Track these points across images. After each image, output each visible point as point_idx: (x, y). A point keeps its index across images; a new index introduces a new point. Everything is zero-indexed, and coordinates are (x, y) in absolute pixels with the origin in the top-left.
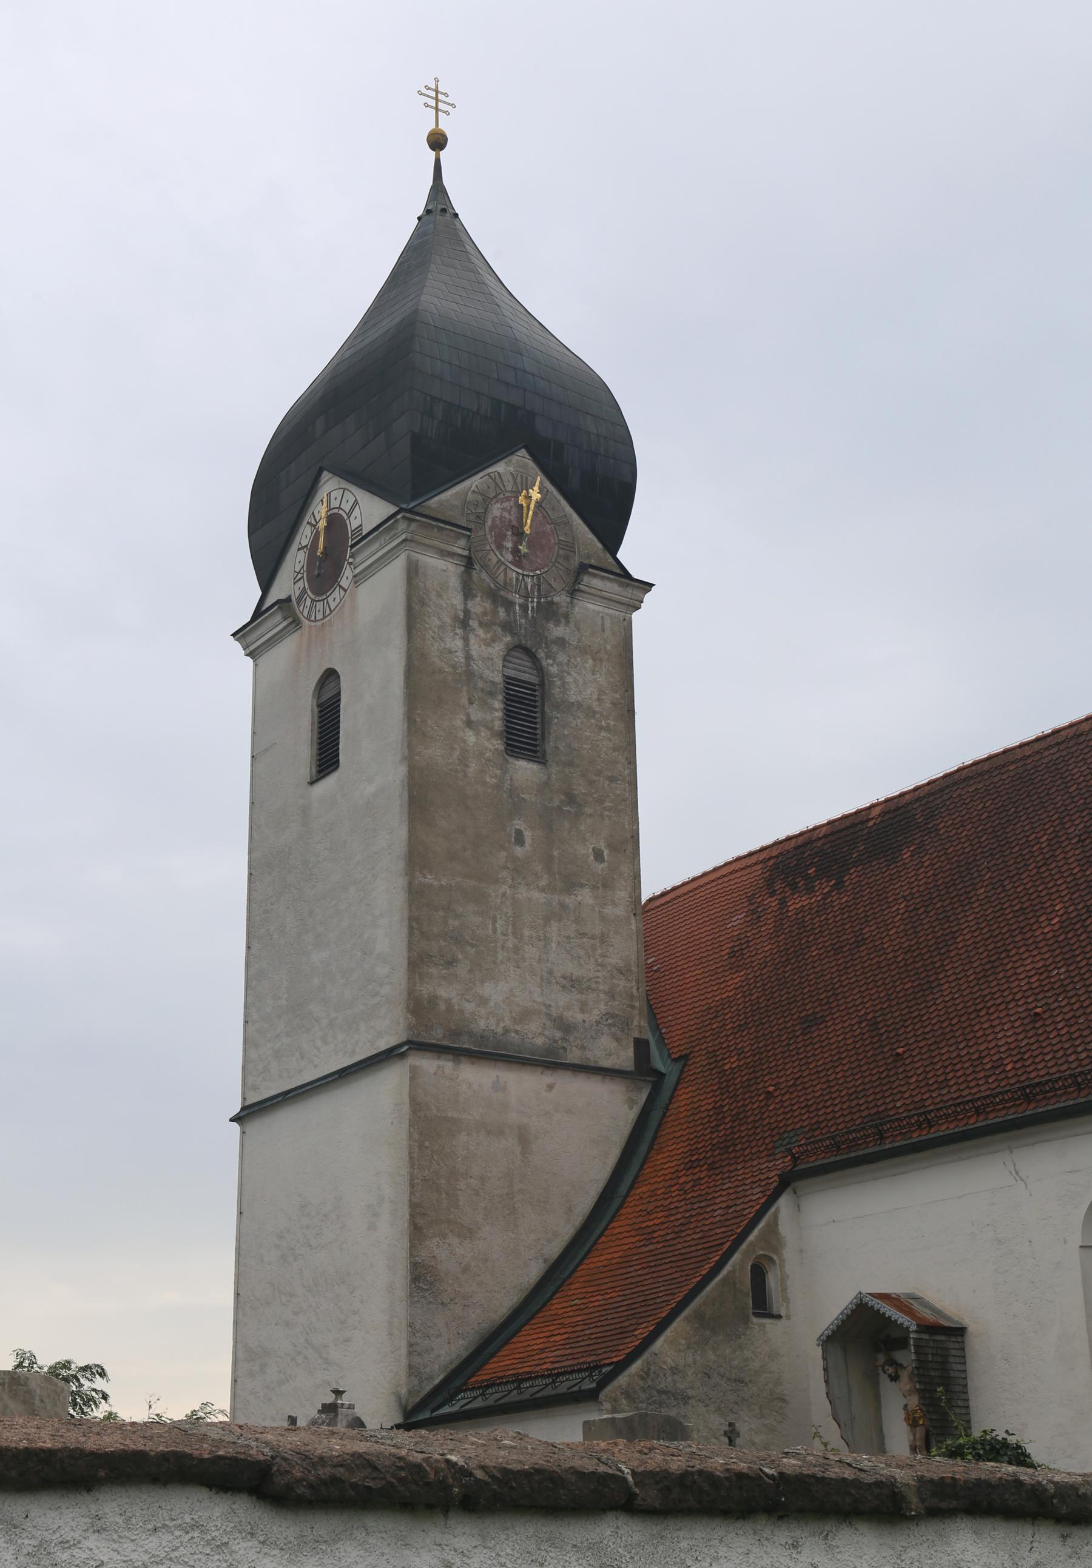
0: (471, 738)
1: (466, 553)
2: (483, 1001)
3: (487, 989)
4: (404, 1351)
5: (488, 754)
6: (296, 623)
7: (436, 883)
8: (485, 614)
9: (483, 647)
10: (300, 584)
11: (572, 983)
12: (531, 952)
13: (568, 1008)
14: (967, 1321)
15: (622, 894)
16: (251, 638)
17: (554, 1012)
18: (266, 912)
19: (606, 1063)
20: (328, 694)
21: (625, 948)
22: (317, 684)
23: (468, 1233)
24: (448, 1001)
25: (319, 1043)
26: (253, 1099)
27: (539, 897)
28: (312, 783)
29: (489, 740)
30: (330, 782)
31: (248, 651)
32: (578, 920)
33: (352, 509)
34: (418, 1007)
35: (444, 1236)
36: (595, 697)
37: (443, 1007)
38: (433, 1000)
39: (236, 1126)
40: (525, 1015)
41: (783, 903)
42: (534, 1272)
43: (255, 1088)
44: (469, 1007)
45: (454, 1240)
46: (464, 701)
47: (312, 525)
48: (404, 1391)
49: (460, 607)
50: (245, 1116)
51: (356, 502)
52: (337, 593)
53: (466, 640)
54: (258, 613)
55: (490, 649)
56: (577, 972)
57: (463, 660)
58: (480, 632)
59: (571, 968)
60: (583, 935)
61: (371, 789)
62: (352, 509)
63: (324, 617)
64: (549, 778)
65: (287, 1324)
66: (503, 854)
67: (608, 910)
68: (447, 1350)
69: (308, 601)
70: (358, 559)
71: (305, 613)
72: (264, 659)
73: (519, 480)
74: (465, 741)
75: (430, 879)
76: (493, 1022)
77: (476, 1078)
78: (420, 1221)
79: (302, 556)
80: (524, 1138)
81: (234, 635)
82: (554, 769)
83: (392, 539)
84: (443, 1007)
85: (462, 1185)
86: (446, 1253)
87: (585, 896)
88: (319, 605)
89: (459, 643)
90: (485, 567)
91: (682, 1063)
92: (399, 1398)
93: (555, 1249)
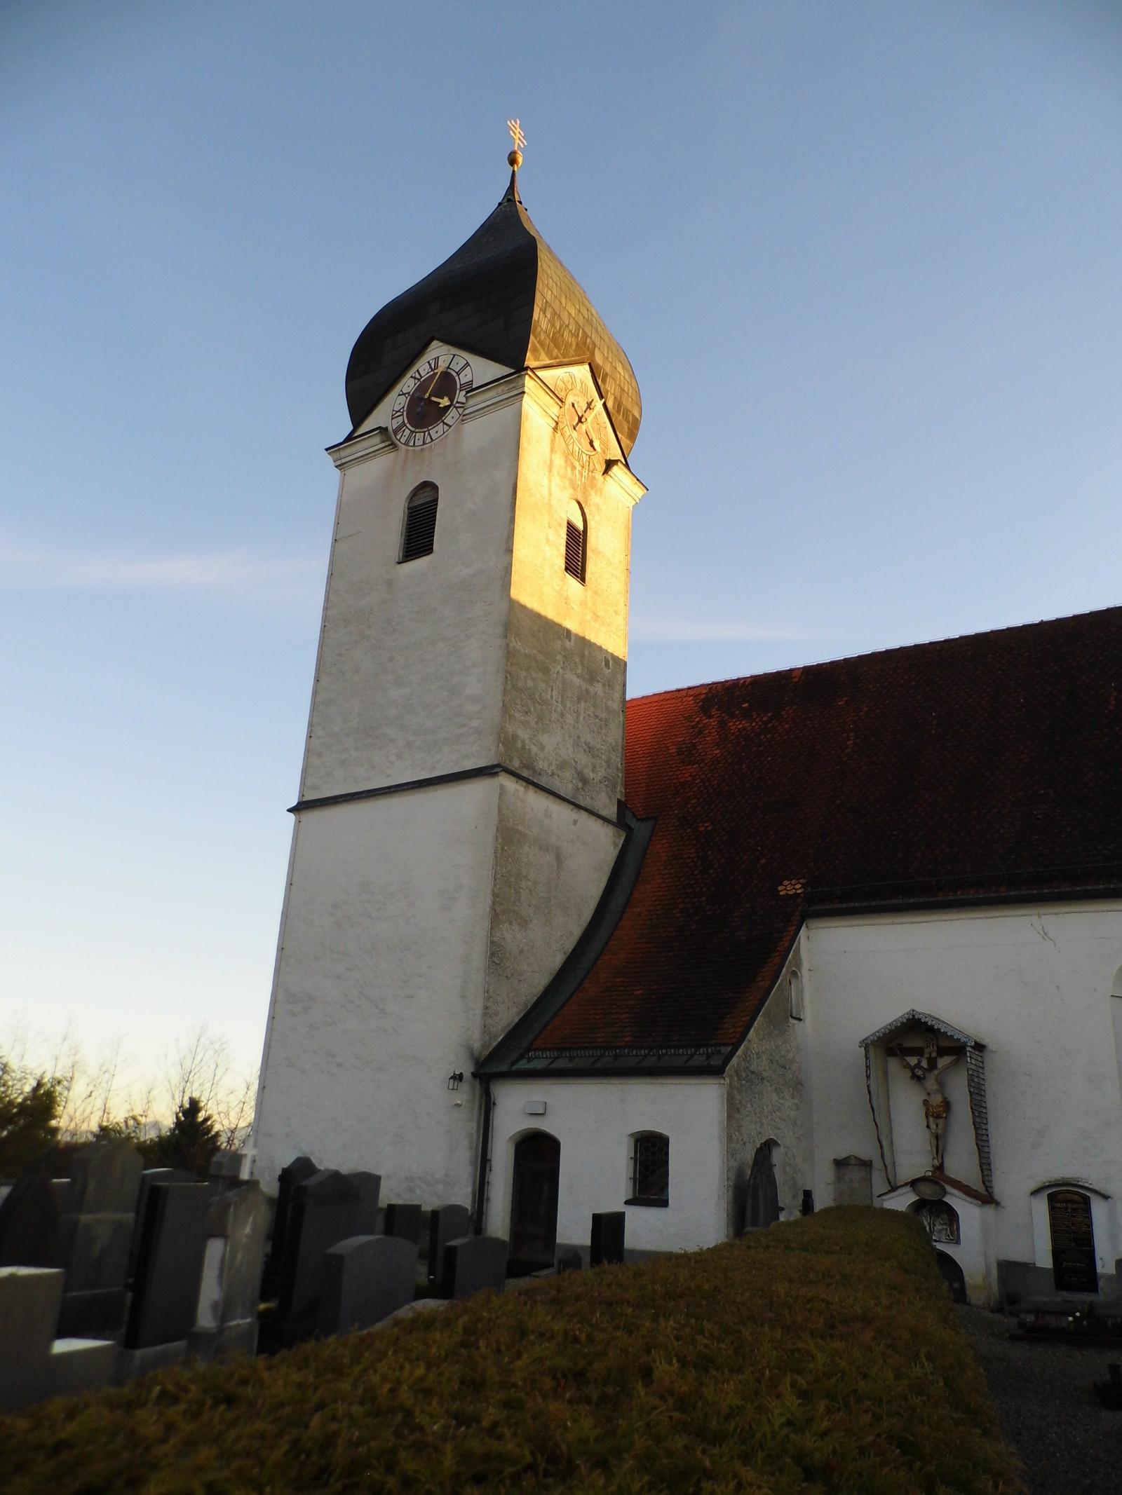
0: (547, 548)
2: (542, 748)
3: (545, 739)
4: (479, 1011)
6: (394, 446)
11: (590, 750)
12: (570, 719)
13: (586, 767)
14: (986, 1041)
15: (617, 695)
16: (343, 453)
17: (579, 767)
18: (340, 655)
19: (604, 813)
20: (419, 500)
21: (615, 734)
23: (524, 923)
24: (523, 742)
25: (393, 758)
26: (311, 796)
27: (577, 681)
30: (421, 563)
31: (339, 463)
32: (595, 706)
33: (463, 368)
34: (507, 741)
35: (511, 923)
37: (519, 745)
38: (515, 737)
39: (292, 816)
40: (562, 766)
41: (722, 723)
42: (558, 961)
43: (314, 788)
44: (534, 749)
45: (516, 927)
48: (477, 1045)
49: (548, 456)
50: (300, 808)
51: (467, 364)
52: (440, 428)
54: (350, 438)
56: (592, 744)
58: (558, 479)
59: (588, 737)
60: (597, 717)
62: (463, 368)
65: (338, 977)
66: (559, 642)
67: (610, 703)
68: (508, 1016)
69: (407, 432)
70: (471, 402)
71: (403, 440)
75: (519, 646)
76: (546, 764)
77: (536, 802)
78: (498, 910)
79: (403, 401)
80: (559, 859)
83: (509, 390)
84: (519, 745)
85: (523, 885)
86: (511, 936)
87: (598, 688)
88: (419, 436)
89: (546, 481)
91: (652, 822)
92: (470, 1050)
93: (570, 945)
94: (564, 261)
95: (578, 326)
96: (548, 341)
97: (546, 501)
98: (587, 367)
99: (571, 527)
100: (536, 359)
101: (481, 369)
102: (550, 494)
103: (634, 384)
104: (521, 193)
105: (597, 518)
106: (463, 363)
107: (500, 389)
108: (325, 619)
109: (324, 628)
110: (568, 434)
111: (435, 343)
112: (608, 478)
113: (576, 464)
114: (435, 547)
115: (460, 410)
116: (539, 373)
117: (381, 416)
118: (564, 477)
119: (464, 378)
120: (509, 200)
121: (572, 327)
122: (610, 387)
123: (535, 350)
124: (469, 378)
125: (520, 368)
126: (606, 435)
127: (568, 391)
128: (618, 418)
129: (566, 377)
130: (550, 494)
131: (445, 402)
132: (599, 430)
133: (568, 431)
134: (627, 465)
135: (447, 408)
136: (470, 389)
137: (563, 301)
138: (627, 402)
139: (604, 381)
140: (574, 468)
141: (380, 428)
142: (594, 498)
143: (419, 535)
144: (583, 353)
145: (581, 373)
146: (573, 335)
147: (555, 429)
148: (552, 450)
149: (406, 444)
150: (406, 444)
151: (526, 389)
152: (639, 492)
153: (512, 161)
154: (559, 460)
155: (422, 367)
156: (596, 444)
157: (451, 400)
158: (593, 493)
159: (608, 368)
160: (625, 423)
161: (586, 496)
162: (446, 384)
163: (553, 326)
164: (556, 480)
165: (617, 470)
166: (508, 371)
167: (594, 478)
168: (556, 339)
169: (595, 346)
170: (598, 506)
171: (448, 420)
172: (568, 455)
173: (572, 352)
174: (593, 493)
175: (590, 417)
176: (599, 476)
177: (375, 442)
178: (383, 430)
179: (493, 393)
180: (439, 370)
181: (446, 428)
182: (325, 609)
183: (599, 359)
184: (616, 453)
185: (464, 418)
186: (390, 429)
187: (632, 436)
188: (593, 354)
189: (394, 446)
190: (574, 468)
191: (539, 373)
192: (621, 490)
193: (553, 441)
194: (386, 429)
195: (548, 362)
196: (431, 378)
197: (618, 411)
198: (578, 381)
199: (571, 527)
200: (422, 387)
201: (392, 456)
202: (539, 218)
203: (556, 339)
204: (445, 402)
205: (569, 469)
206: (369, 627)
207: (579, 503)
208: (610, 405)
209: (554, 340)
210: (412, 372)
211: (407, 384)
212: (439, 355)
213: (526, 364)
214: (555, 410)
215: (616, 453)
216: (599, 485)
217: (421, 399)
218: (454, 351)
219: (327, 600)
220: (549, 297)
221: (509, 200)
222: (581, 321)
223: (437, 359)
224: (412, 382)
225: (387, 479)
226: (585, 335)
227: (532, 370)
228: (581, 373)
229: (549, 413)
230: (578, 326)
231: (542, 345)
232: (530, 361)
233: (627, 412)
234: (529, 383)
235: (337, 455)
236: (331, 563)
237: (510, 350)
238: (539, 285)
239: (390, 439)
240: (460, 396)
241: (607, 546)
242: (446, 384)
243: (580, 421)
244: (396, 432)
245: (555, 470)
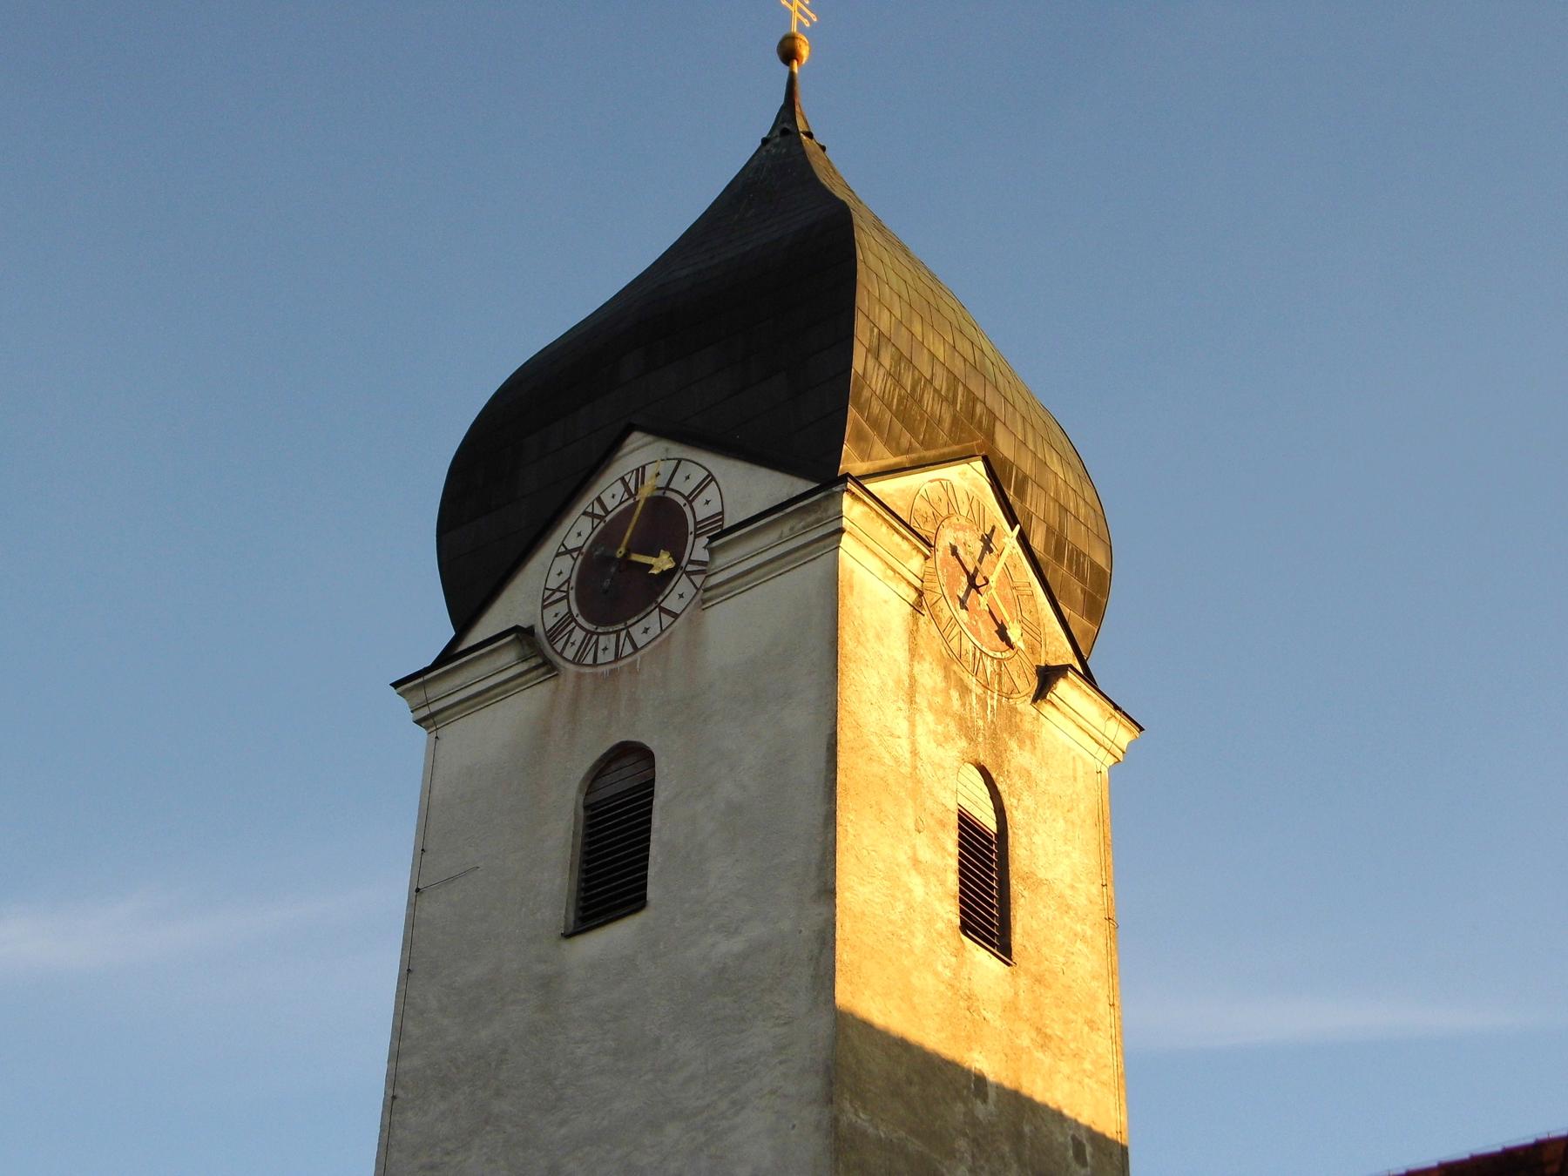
0: (916, 883)
1: (918, 583)
5: (940, 926)
7: (871, 1130)
8: (934, 691)
9: (933, 745)
10: (562, 608)
16: (435, 690)
22: (595, 766)
28: (568, 936)
29: (941, 901)
30: (618, 935)
31: (424, 712)
33: (701, 487)
36: (1068, 880)
46: (910, 823)
47: (593, 515)
49: (905, 668)
51: (710, 478)
52: (653, 620)
53: (912, 725)
55: (941, 751)
57: (908, 755)
58: (930, 717)
61: (737, 944)
62: (701, 487)
63: (618, 657)
64: (1016, 994)
66: (959, 1107)
69: (578, 635)
70: (721, 560)
71: (570, 653)
72: (457, 732)
73: (975, 505)
74: (910, 891)
75: (862, 1120)
81: (396, 685)
82: (1023, 982)
83: (808, 528)
88: (608, 641)
89: (902, 726)
90: (934, 617)
94: (913, 250)
95: (954, 379)
96: (888, 415)
97: (906, 770)
98: (979, 465)
99: (967, 824)
100: (865, 456)
101: (742, 488)
102: (914, 753)
103: (1089, 494)
104: (810, 114)
105: (1028, 801)
106: (698, 475)
107: (786, 529)
108: (393, 1080)
109: (392, 1103)
110: (946, 614)
111: (636, 438)
112: (1047, 709)
113: (972, 682)
114: (652, 892)
115: (698, 579)
116: (872, 486)
117: (517, 604)
118: (942, 712)
119: (703, 509)
120: (785, 132)
121: (941, 382)
122: (1035, 504)
123: (860, 437)
124: (715, 507)
125: (829, 480)
126: (1035, 611)
127: (939, 521)
128: (1060, 573)
129: (935, 491)
130: (914, 753)
131: (663, 562)
132: (1018, 599)
133: (948, 609)
134: (1088, 677)
135: (667, 575)
136: (720, 532)
137: (917, 328)
138: (1077, 536)
139: (1021, 493)
140: (964, 690)
141: (516, 629)
142: (1019, 757)
143: (612, 865)
144: (968, 437)
145: (969, 477)
146: (944, 399)
147: (917, 607)
148: (914, 653)
149: (577, 661)
150: (577, 661)
151: (845, 523)
152: (1122, 735)
153: (788, 53)
154: (930, 676)
155: (609, 491)
156: (1014, 633)
157: (677, 557)
158: (1013, 745)
159: (1027, 465)
160: (1076, 580)
161: (998, 752)
162: (663, 521)
163: (898, 382)
164: (927, 721)
165: (1067, 690)
166: (802, 486)
167: (1013, 710)
168: (906, 411)
169: (995, 418)
170: (1027, 774)
171: (672, 603)
172: (951, 661)
173: (943, 437)
174: (1013, 745)
175: (994, 572)
176: (1024, 705)
177: (507, 660)
178: (522, 635)
179: (771, 536)
180: (645, 492)
181: (667, 619)
182: (396, 1056)
183: (1005, 446)
184: (1059, 651)
185: (705, 598)
186: (539, 630)
187: (1095, 609)
188: (990, 436)
189: (549, 668)
190: (964, 690)
191: (872, 486)
192: (1076, 739)
193: (913, 634)
194: (530, 631)
195: (891, 460)
196: (629, 511)
197: (1058, 556)
198: (961, 496)
199: (967, 824)
200: (609, 534)
201: (543, 691)
202: (850, 160)
203: (906, 411)
204: (663, 562)
205: (955, 694)
206: (498, 1094)
207: (983, 771)
208: (1037, 542)
209: (903, 415)
210: (585, 503)
211: (577, 530)
212: (645, 464)
213: (844, 467)
214: (916, 563)
215: (1059, 651)
216: (1027, 726)
217: (610, 560)
218: (677, 451)
219: (399, 1033)
220: (885, 321)
221: (785, 132)
222: (959, 367)
223: (640, 472)
224: (585, 525)
225: (534, 743)
226: (972, 399)
227: (857, 480)
228: (969, 477)
229: (897, 569)
230: (954, 379)
231: (875, 424)
232: (851, 462)
233: (1077, 555)
234: (852, 510)
235: (420, 696)
236: (409, 944)
237: (805, 438)
238: (862, 300)
239: (540, 652)
240: (698, 550)
241: (1057, 863)
242: (663, 521)
243: (972, 584)
244: (552, 635)
245: (921, 700)
